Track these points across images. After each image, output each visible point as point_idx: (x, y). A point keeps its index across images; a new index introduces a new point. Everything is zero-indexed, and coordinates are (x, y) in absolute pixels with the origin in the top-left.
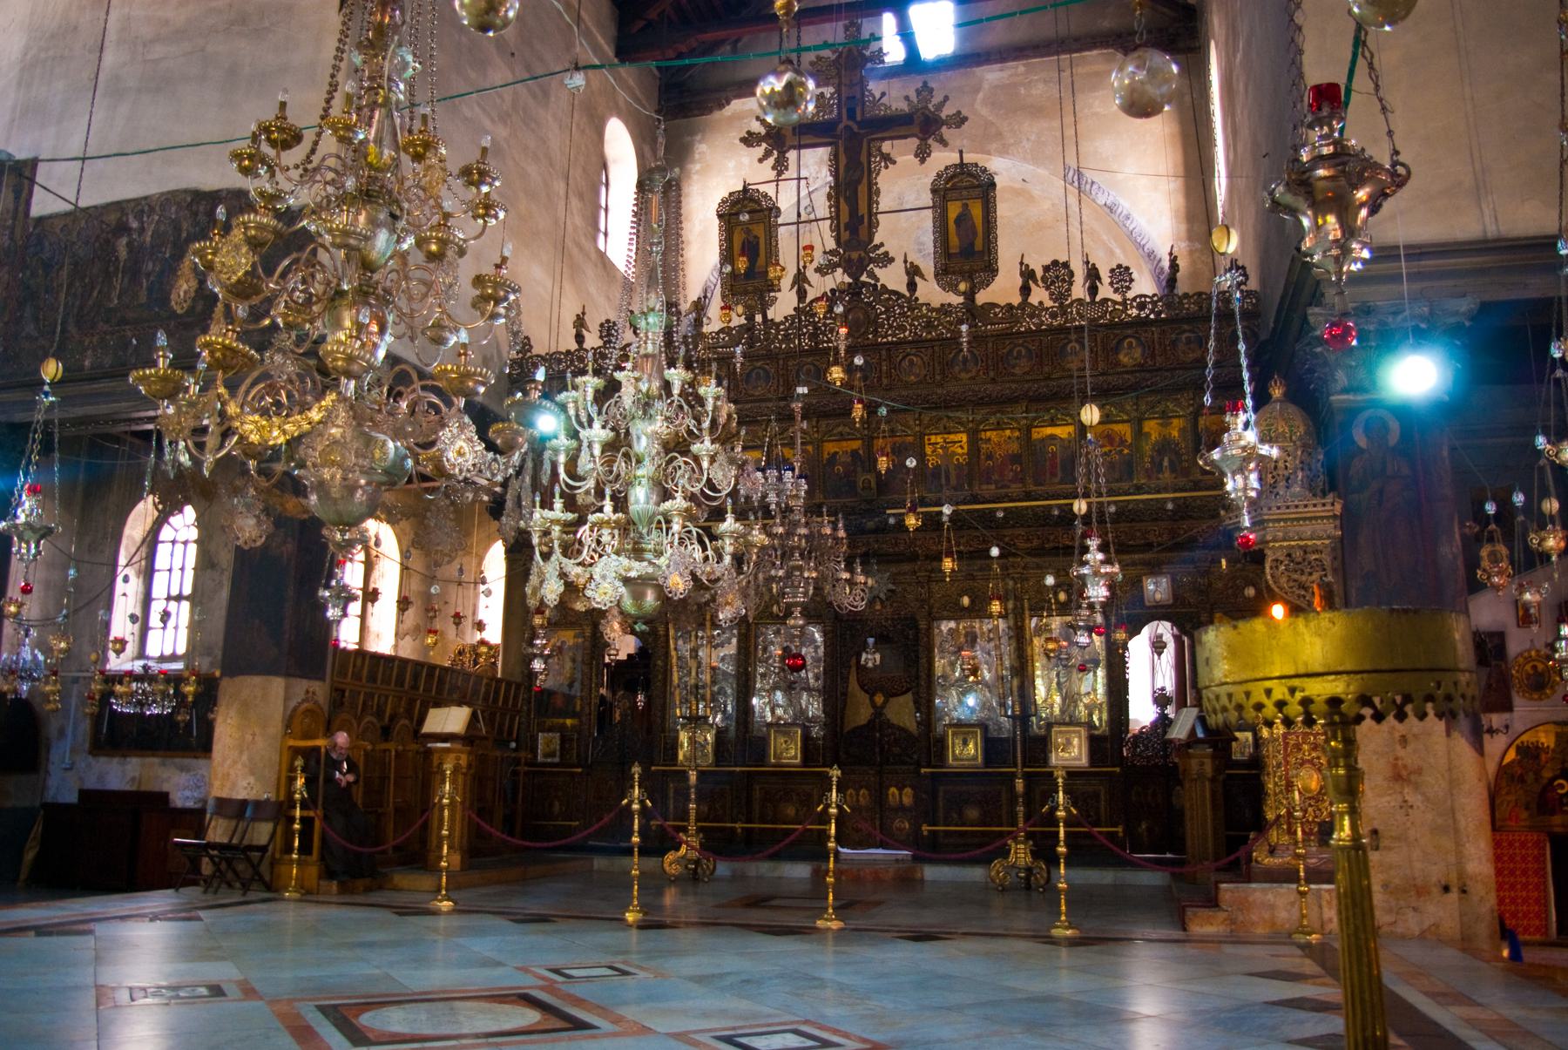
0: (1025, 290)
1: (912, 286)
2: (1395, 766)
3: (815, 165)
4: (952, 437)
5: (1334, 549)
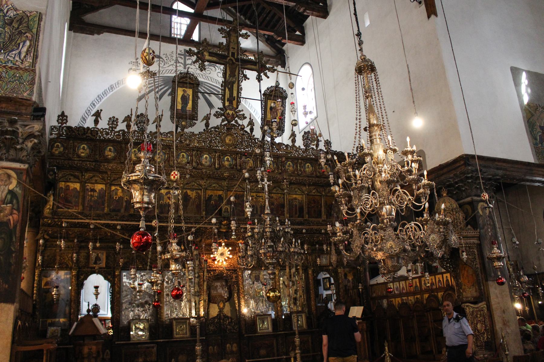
2: (503, 320)
5: (477, 248)
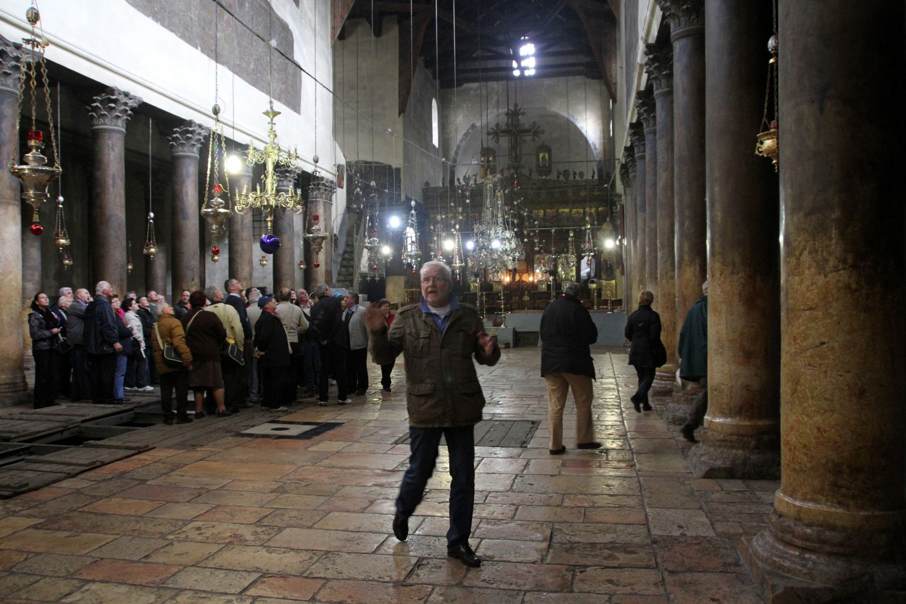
0: (558, 177)
1: (530, 174)
3: (505, 142)
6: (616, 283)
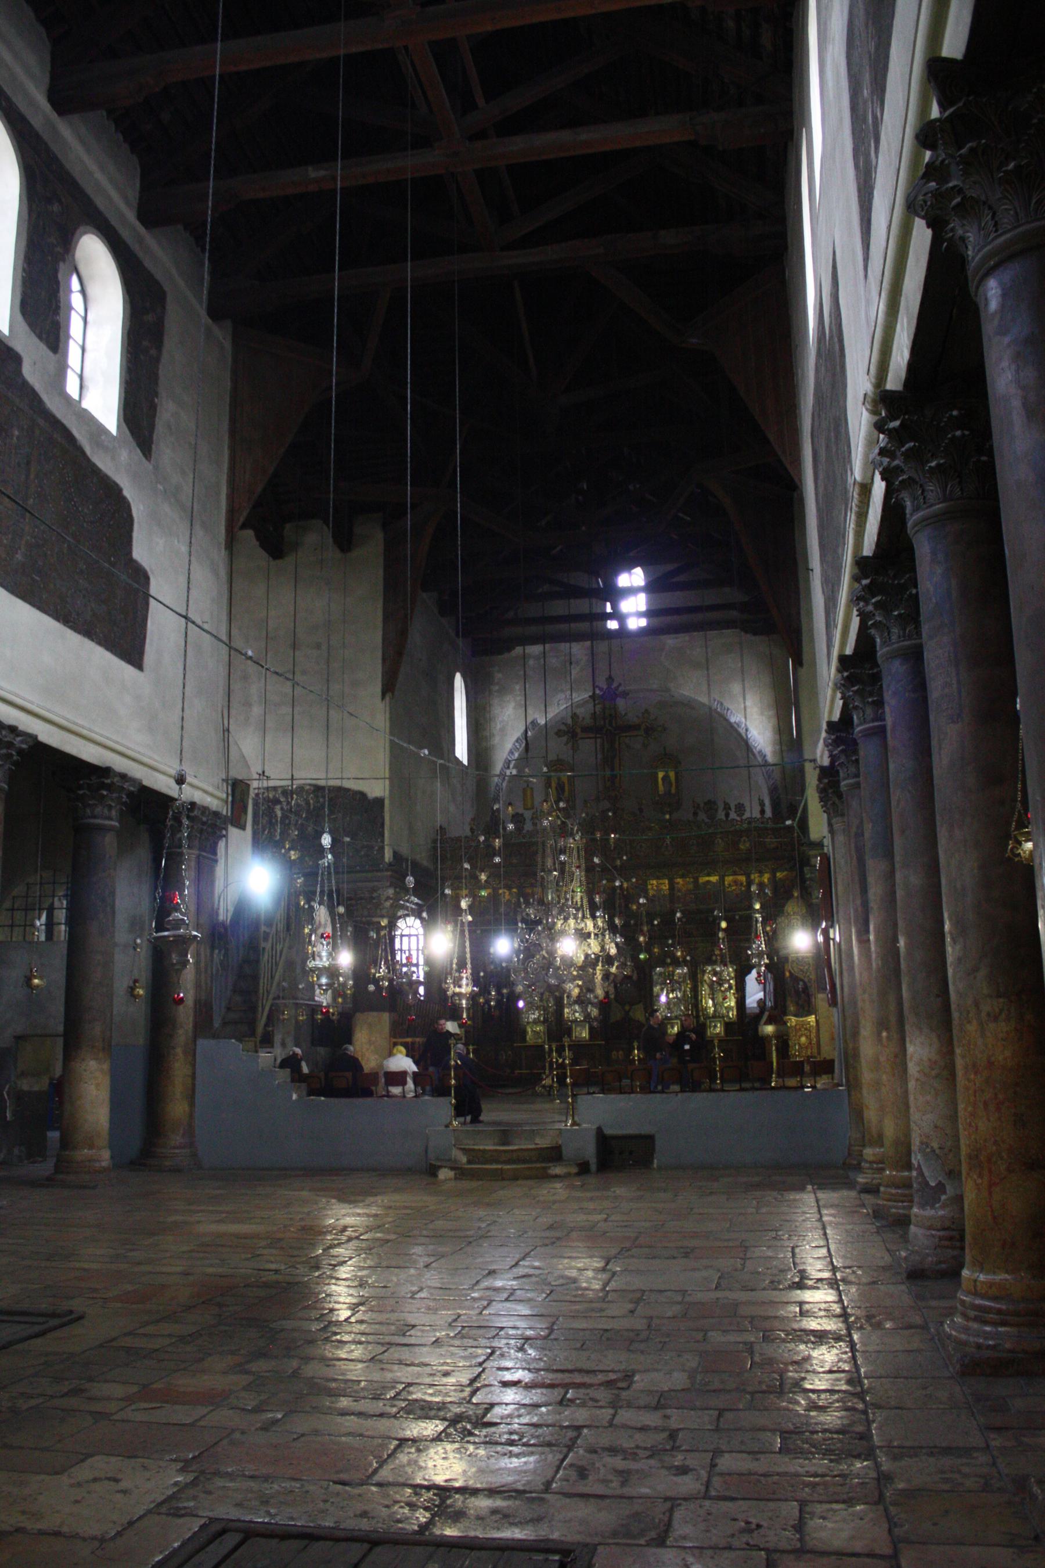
0: (695, 814)
4: (661, 881)
6: (817, 1021)
